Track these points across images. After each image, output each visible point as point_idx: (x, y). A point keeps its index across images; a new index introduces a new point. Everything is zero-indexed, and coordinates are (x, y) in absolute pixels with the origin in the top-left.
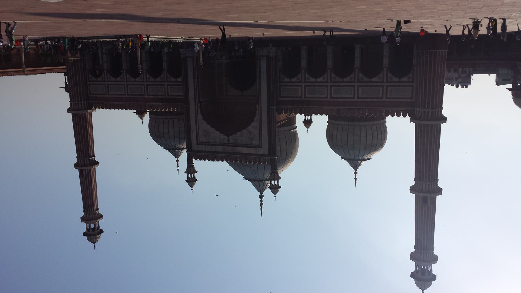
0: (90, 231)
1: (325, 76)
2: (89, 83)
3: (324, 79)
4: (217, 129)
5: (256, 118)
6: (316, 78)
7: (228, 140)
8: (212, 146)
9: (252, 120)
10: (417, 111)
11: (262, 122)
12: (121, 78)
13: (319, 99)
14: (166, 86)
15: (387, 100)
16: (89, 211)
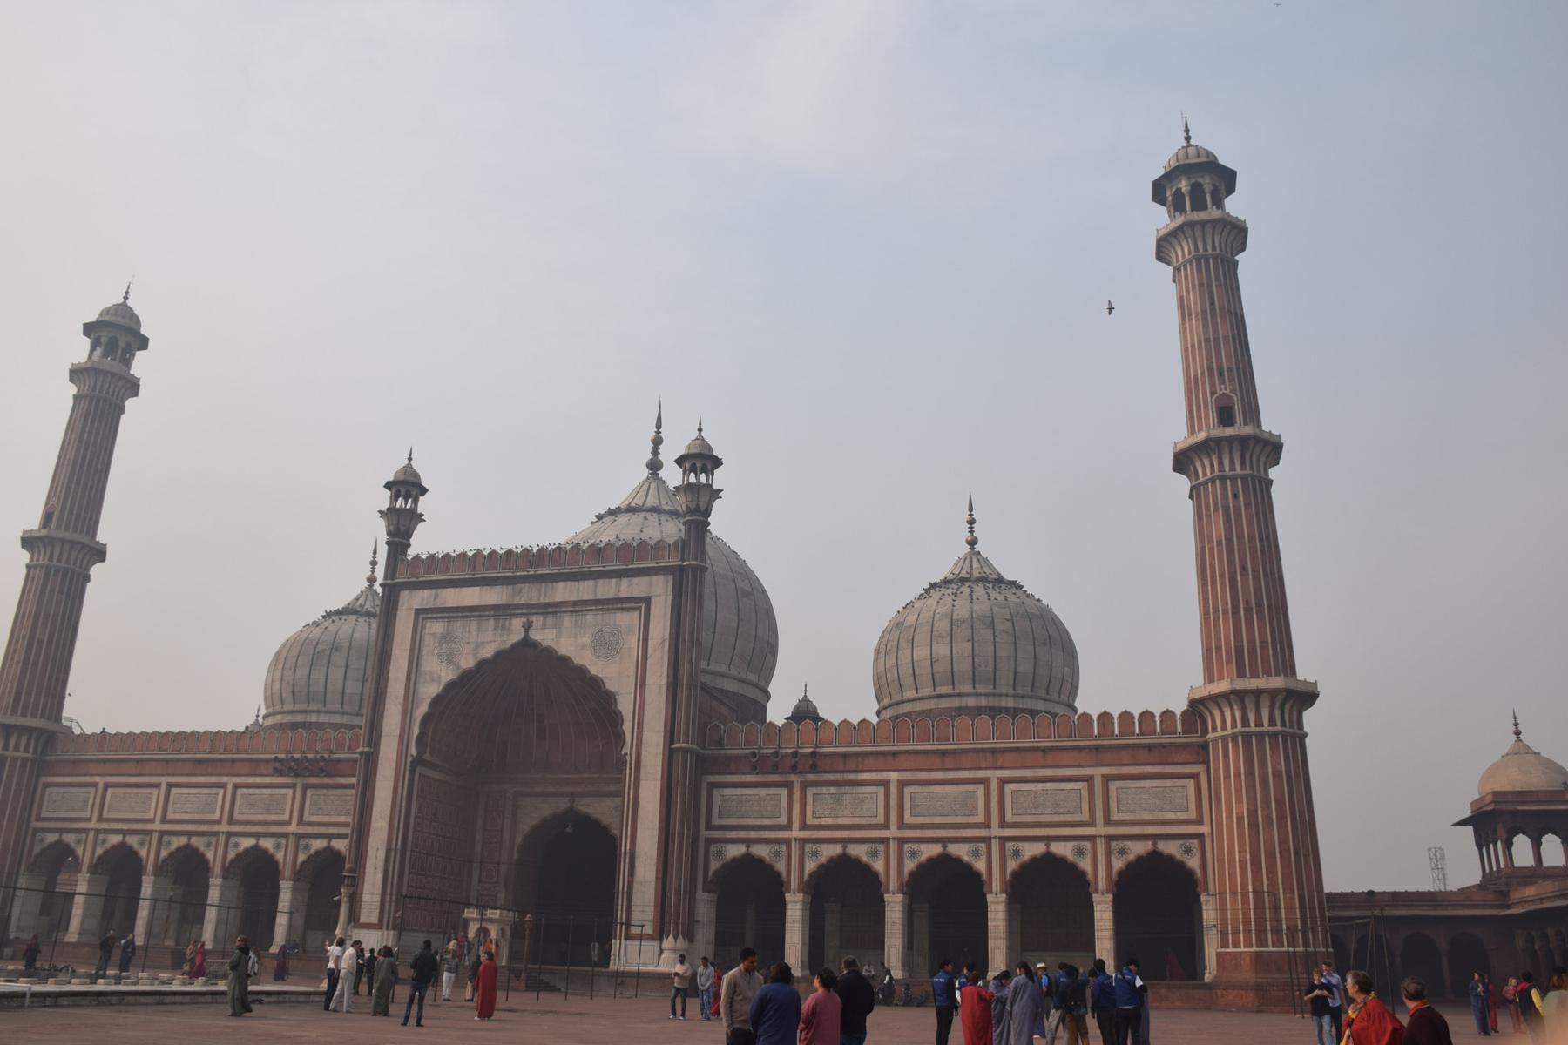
0: (1189, 188)
1: (231, 855)
2: (1204, 829)
3: (236, 845)
4: (565, 660)
5: (422, 710)
6: (256, 848)
7: (528, 626)
8: (591, 597)
9: (436, 701)
10: (26, 750)
11: (402, 698)
12: (1017, 853)
13: (259, 780)
14: (796, 824)
15: (97, 779)
16: (1191, 262)
